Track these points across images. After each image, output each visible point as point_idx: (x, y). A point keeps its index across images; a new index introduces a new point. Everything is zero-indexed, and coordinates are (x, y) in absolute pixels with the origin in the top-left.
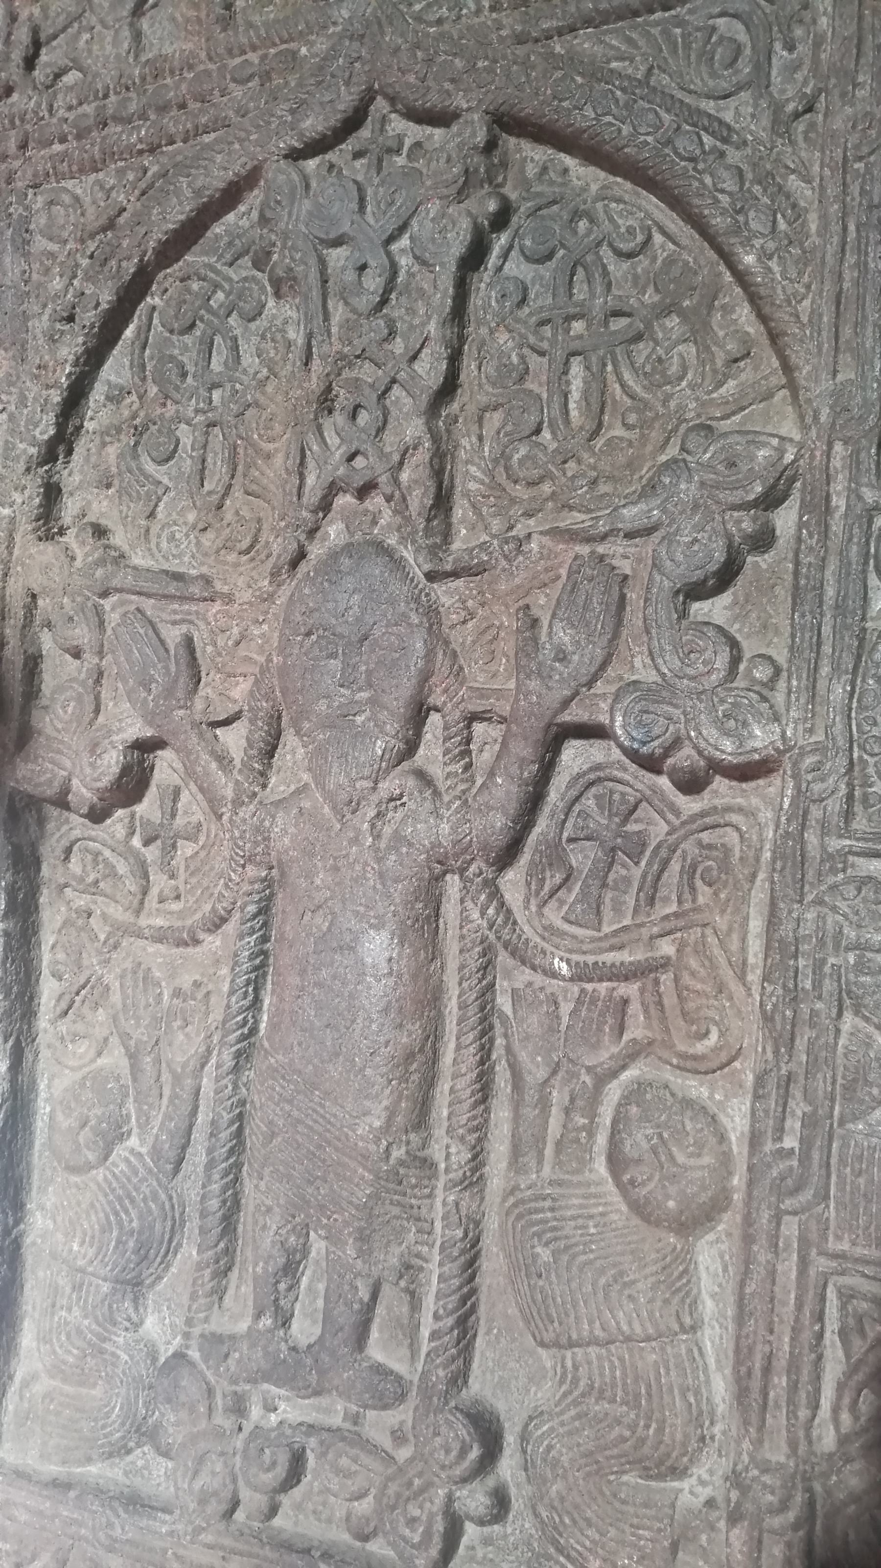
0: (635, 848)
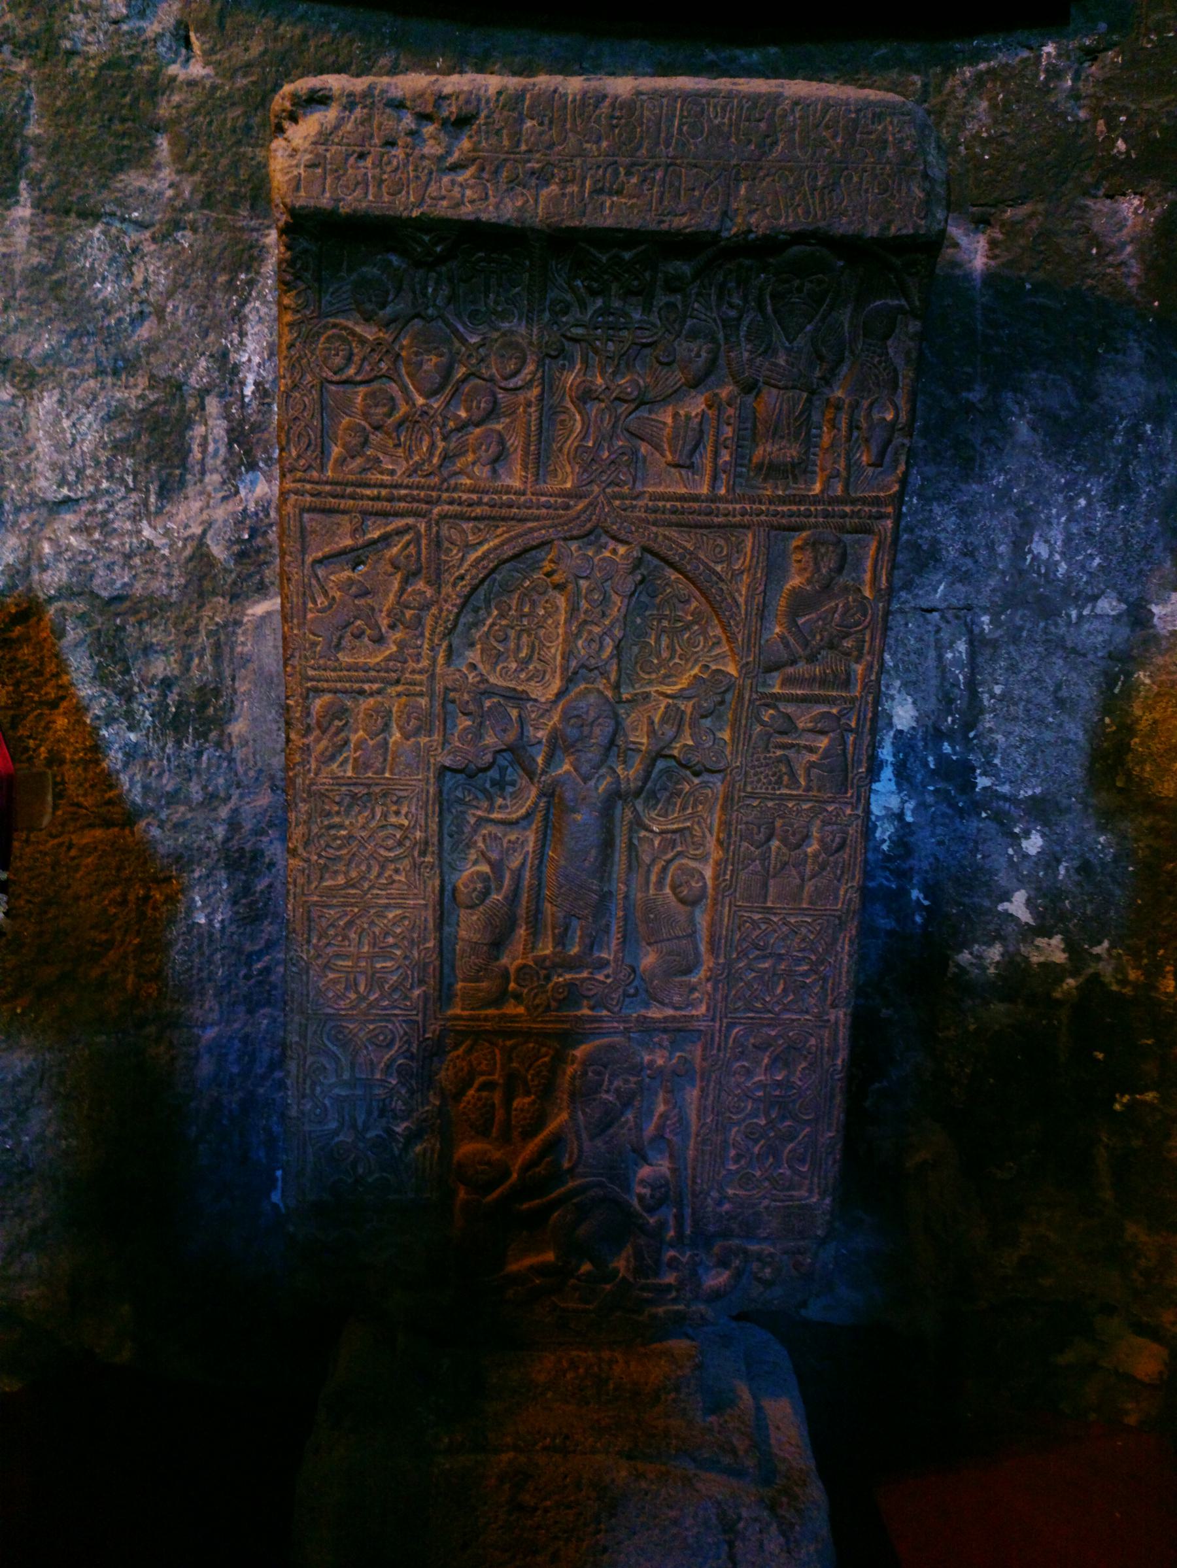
0: (678, 793)
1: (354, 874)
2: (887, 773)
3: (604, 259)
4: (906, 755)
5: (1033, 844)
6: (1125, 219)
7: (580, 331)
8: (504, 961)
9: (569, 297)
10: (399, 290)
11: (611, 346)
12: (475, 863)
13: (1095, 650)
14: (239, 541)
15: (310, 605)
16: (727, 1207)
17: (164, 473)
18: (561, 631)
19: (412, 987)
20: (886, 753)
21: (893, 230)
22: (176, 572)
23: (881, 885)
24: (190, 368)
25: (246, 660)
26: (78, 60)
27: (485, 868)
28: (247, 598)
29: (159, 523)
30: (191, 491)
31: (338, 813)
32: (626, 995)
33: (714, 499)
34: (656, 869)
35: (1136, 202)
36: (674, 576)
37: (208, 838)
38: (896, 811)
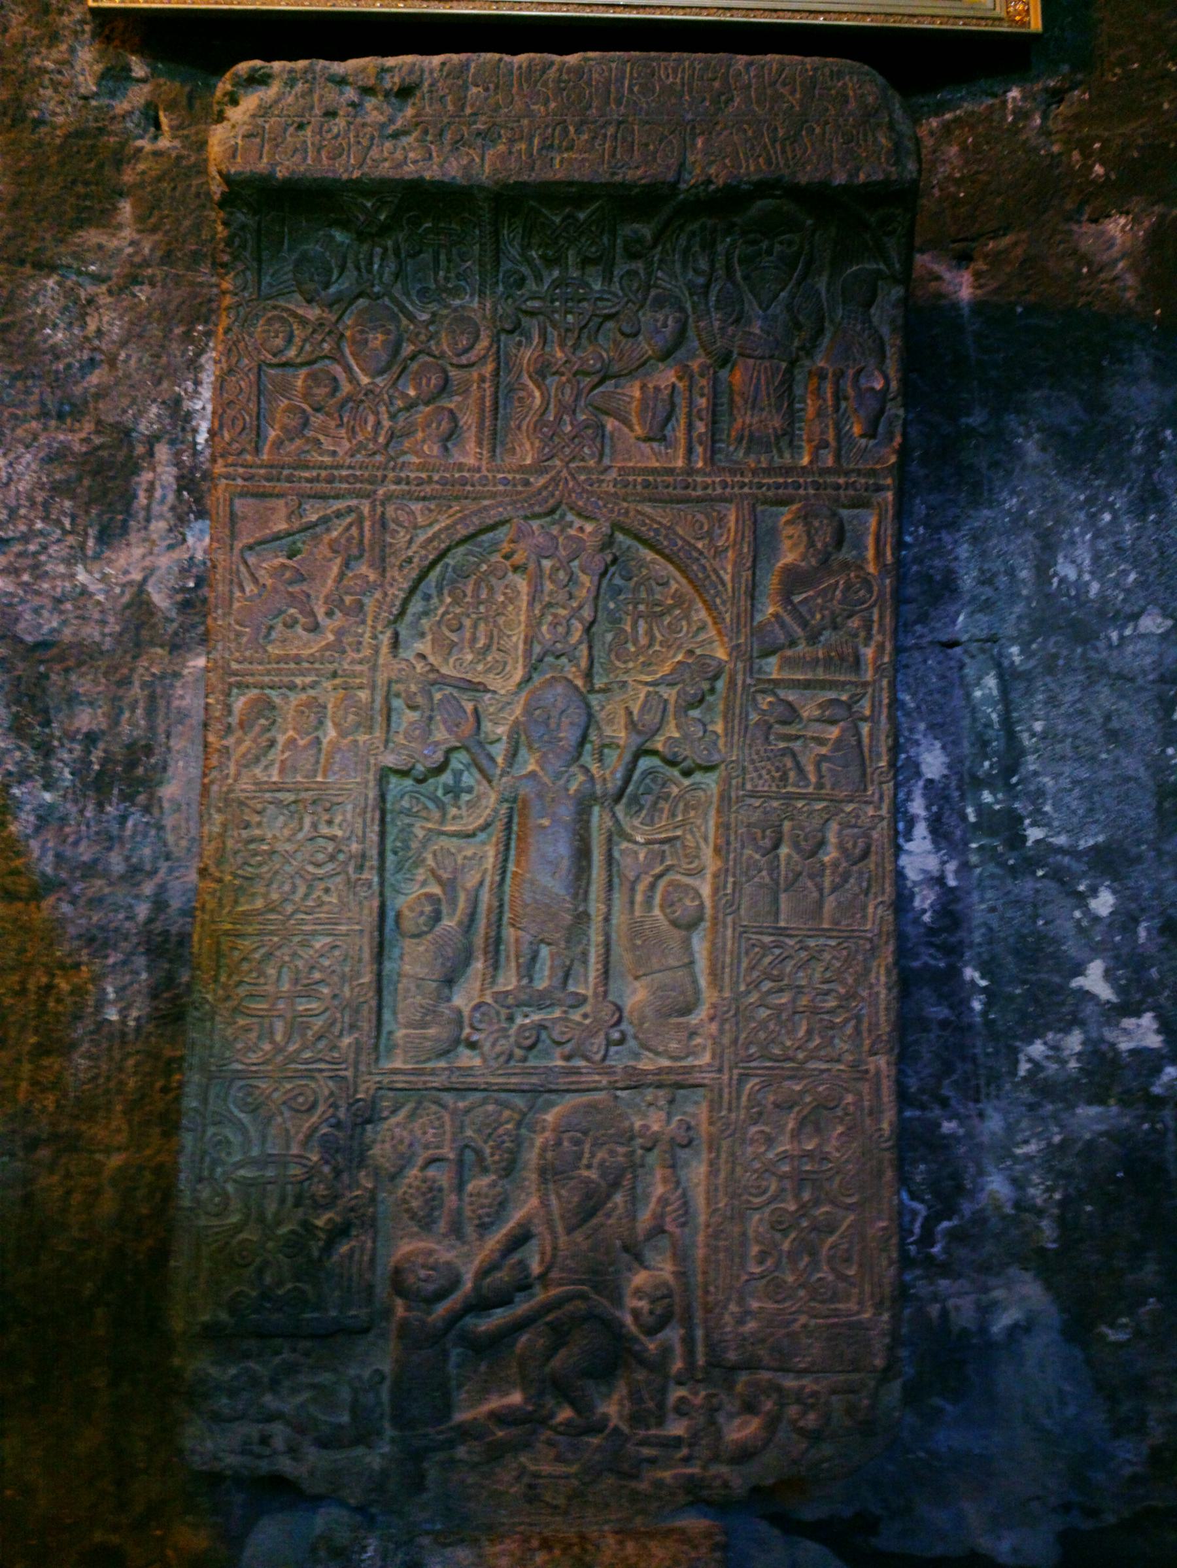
0: (666, 798)
1: (275, 896)
2: (921, 829)
3: (558, 220)
4: (941, 808)
5: (1104, 903)
6: (1113, 238)
7: (537, 304)
8: (459, 1000)
9: (525, 270)
10: (343, 268)
11: (570, 318)
12: (424, 884)
13: (1144, 673)
14: (184, 590)
16: (751, 1325)
17: (106, 517)
18: (523, 618)
19: (341, 1035)
20: (917, 807)
21: (862, 177)
22: (112, 620)
23: (926, 964)
24: (140, 414)
25: (183, 715)
26: (43, 130)
27: (436, 890)
28: (189, 650)
29: (95, 567)
30: (133, 537)
31: (259, 824)
32: (609, 1043)
33: (690, 471)
34: (641, 887)
35: (1122, 221)
36: (648, 555)
37: (127, 918)
38: (936, 874)
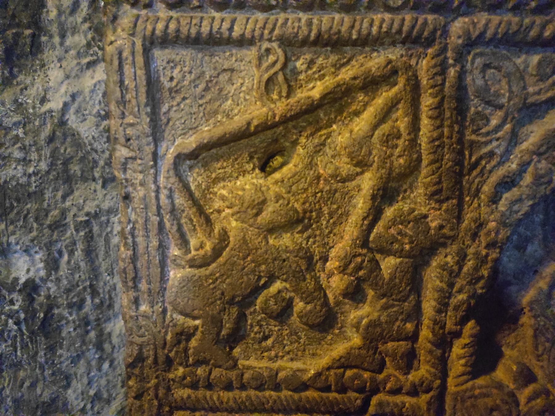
15: (175, 251)
30: (49, 55)
